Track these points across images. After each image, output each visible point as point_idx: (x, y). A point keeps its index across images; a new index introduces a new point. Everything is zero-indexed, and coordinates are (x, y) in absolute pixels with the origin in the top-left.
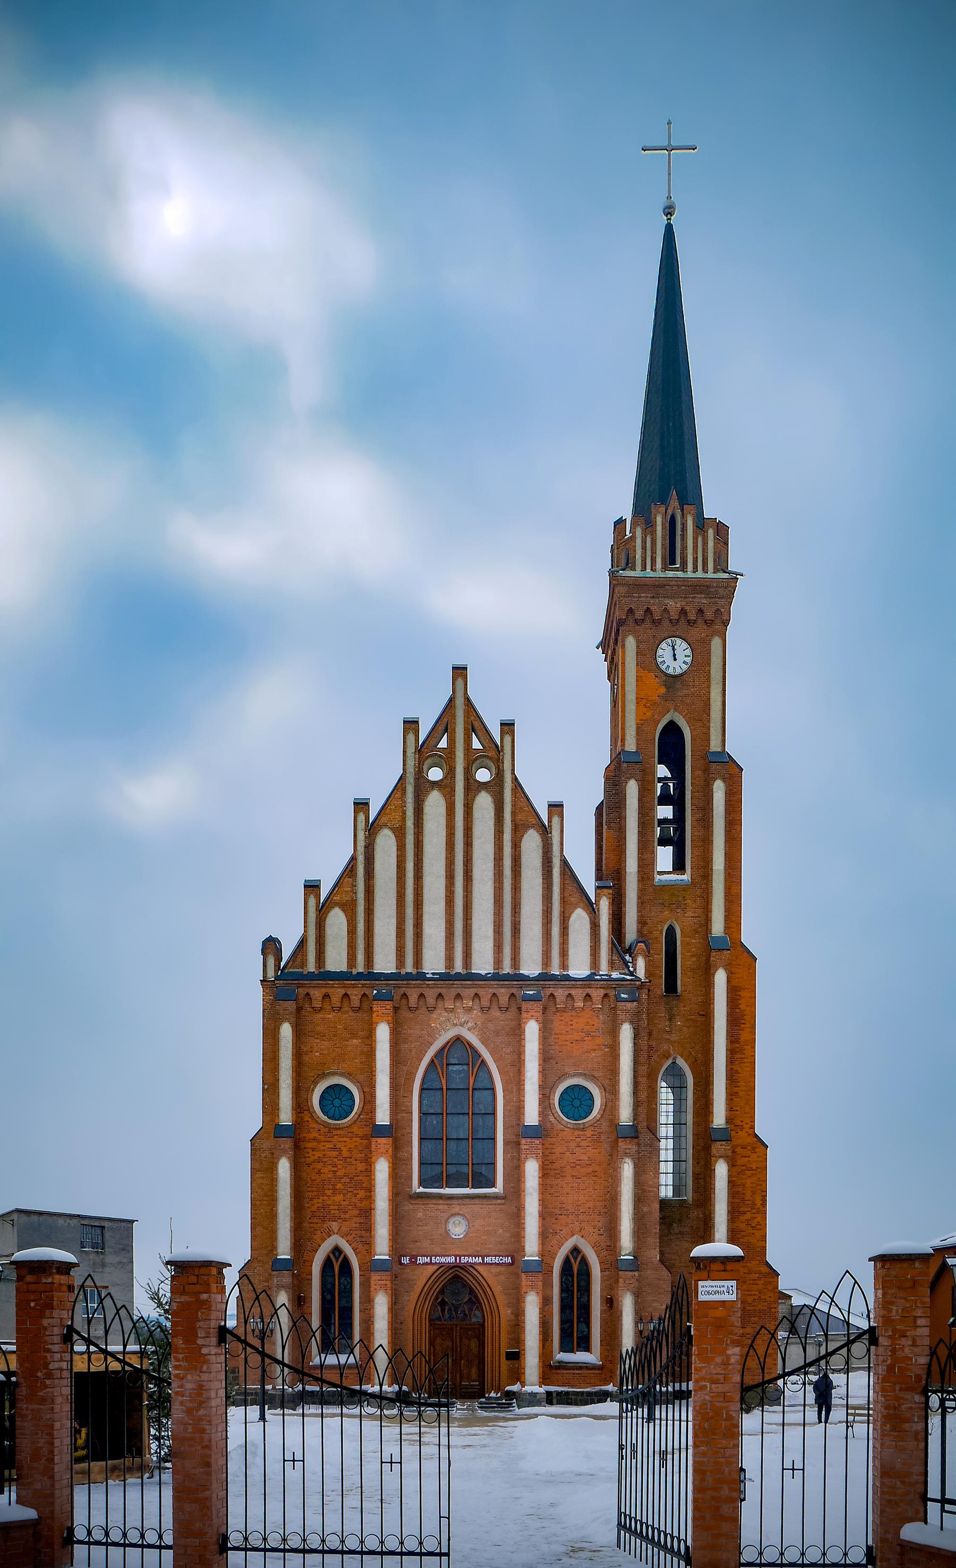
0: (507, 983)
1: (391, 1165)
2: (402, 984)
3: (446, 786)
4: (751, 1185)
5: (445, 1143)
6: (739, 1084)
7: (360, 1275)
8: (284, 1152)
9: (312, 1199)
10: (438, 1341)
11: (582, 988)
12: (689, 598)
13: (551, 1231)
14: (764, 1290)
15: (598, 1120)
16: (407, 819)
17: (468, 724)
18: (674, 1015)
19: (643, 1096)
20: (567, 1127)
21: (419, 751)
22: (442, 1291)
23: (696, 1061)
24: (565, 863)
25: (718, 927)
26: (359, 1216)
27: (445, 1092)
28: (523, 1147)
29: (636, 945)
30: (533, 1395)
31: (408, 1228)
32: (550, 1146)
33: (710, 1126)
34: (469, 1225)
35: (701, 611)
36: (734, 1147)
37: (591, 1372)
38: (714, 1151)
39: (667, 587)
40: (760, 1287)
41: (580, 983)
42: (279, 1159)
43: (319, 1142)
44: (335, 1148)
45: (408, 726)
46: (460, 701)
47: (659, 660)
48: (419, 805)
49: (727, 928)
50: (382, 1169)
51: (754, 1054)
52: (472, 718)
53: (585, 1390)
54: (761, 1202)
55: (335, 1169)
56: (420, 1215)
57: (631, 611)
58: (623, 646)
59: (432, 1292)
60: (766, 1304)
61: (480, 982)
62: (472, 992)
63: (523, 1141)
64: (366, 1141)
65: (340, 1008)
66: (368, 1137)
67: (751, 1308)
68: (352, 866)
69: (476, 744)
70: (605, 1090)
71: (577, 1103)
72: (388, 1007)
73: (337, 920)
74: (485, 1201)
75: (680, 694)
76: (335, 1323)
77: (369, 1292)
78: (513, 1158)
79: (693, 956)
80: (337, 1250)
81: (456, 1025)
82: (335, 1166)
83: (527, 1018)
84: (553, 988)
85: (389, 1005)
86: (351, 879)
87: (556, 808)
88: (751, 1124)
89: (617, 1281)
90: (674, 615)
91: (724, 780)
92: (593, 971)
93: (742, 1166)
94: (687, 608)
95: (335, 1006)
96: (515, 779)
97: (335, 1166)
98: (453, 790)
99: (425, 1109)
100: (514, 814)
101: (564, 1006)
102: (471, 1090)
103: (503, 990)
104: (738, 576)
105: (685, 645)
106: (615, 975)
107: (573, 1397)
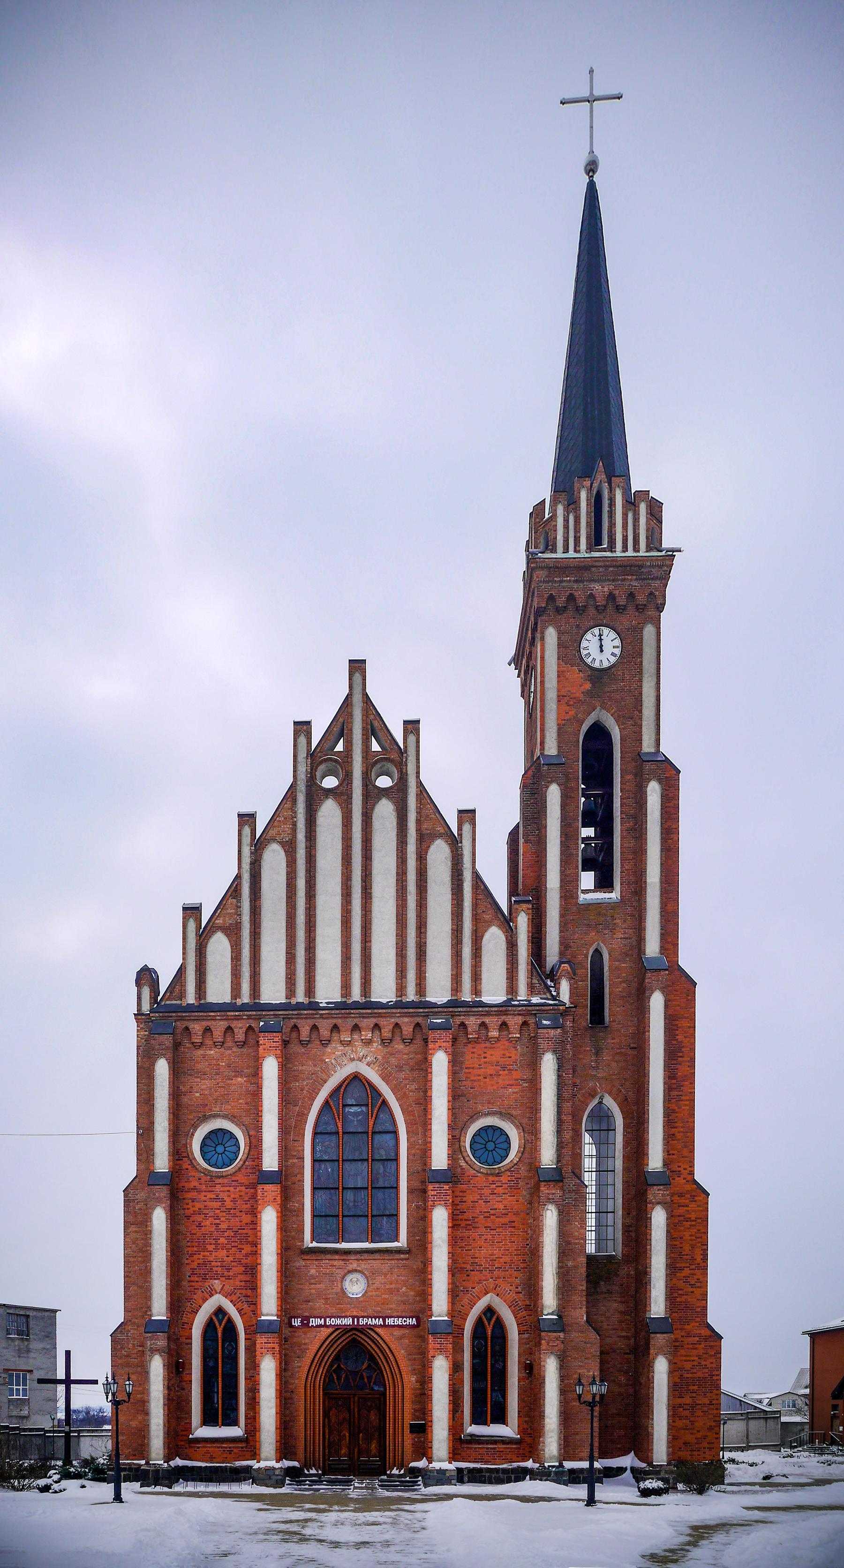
0: (411, 1010)
1: (279, 1214)
2: (293, 1014)
3: (342, 794)
4: (690, 1238)
5: (341, 1193)
6: (677, 1125)
7: (246, 1339)
8: (159, 1201)
9: (192, 1255)
10: (333, 1412)
11: (495, 1015)
12: (618, 580)
13: (462, 1289)
14: (704, 1356)
15: (516, 1164)
16: (298, 830)
17: (367, 724)
18: (602, 1049)
19: (568, 1135)
20: (480, 1173)
21: (312, 755)
22: (337, 1358)
23: (627, 1099)
24: (477, 877)
25: (652, 947)
26: (245, 1273)
27: (341, 1136)
28: (431, 1193)
29: (560, 966)
30: (442, 1472)
31: (300, 1286)
32: (461, 1194)
33: (645, 1170)
34: (368, 1283)
35: (631, 596)
36: (672, 1195)
37: (508, 1446)
38: (650, 1197)
39: (593, 569)
40: (701, 1352)
41: (496, 1009)
42: (153, 1209)
43: (199, 1191)
44: (217, 1199)
45: (299, 727)
46: (357, 699)
47: (584, 652)
48: (311, 816)
49: (663, 949)
50: (269, 1219)
51: (693, 1090)
52: (372, 717)
53: (501, 1467)
55: (217, 1221)
56: (313, 1272)
57: (551, 598)
58: (543, 639)
59: (326, 1358)
60: (706, 1370)
61: (380, 1011)
62: (372, 1021)
63: (430, 1187)
65: (223, 1043)
66: (253, 1186)
67: (690, 1375)
68: (237, 885)
69: (375, 747)
70: (523, 1130)
71: (491, 1146)
72: (276, 1039)
73: (219, 946)
74: (387, 1256)
75: (607, 689)
77: (255, 1356)
78: (418, 1207)
79: (623, 982)
80: (220, 1311)
81: (352, 1060)
82: (218, 1218)
83: (434, 1049)
84: (464, 1015)
85: (277, 1037)
86: (235, 900)
87: (467, 816)
88: (690, 1169)
89: (538, 1344)
90: (600, 601)
91: (660, 781)
92: (510, 997)
93: (679, 1216)
94: (617, 592)
95: (217, 1040)
96: (420, 784)
97: (218, 1218)
98: (350, 798)
99: (318, 1156)
100: (418, 822)
101: (477, 1036)
102: (370, 1134)
103: (406, 1020)
104: (674, 554)
105: (613, 635)
106: (535, 1000)
107: (487, 1475)
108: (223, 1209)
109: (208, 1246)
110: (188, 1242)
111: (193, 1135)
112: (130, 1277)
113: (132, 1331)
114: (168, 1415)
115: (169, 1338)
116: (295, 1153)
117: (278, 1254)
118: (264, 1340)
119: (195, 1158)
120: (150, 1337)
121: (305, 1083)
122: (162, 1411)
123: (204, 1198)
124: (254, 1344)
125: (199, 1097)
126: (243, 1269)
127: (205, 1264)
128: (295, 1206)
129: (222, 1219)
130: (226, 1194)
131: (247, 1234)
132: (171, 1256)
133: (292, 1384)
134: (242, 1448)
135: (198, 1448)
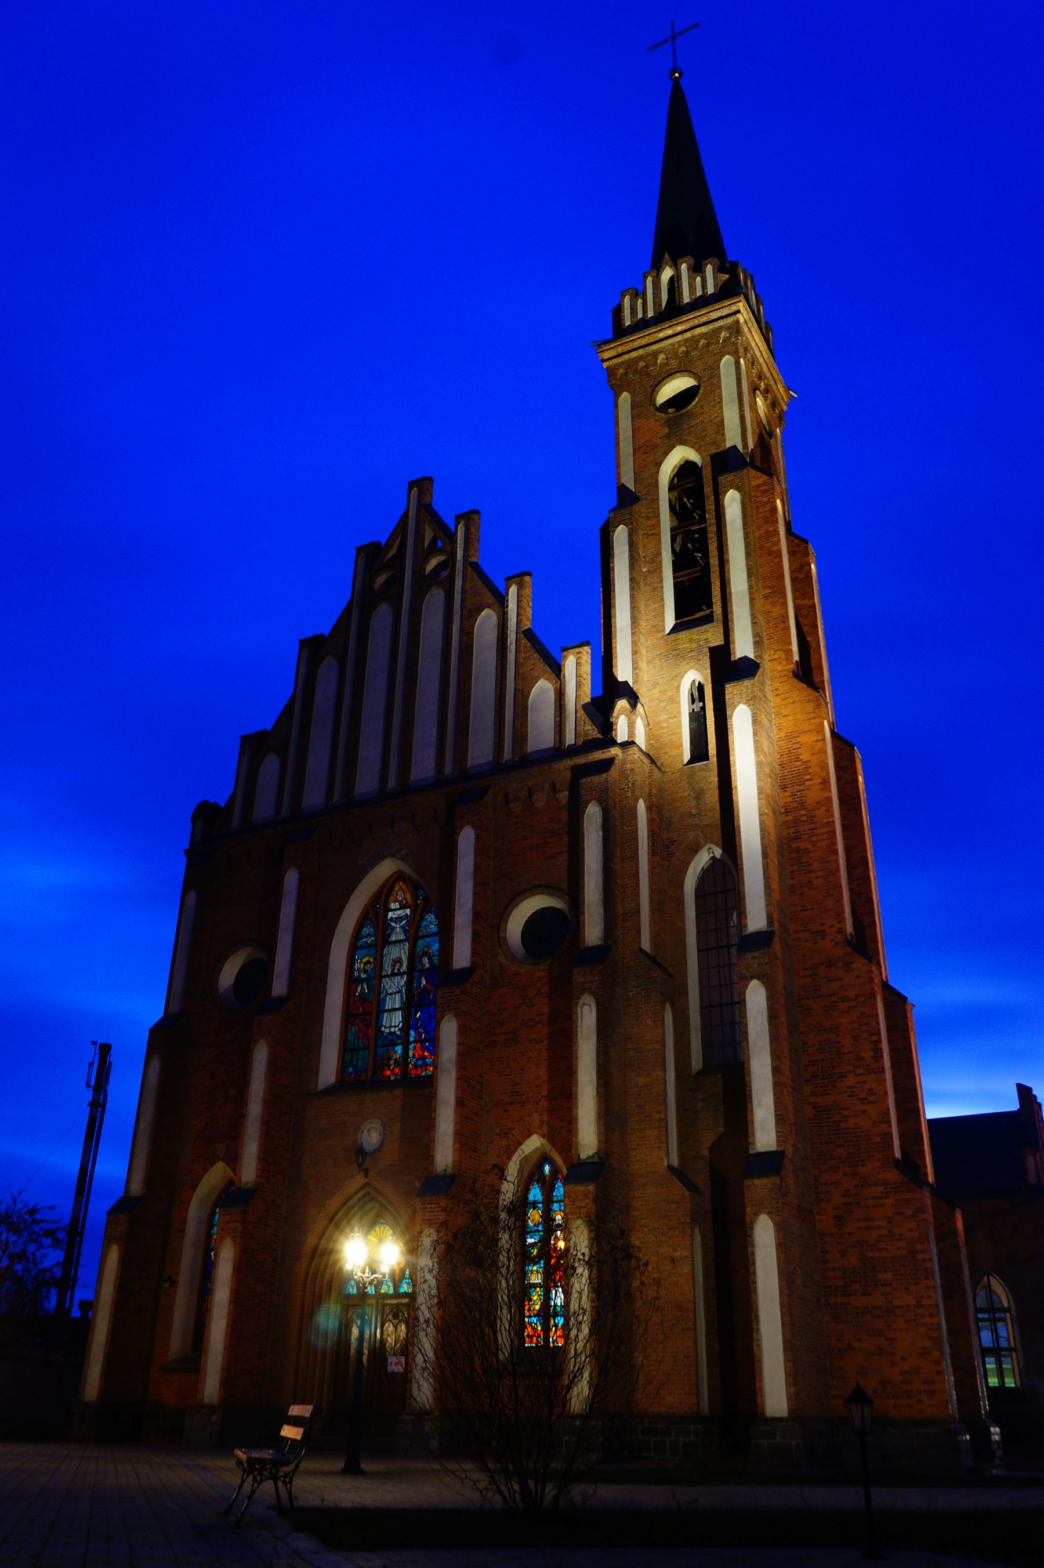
54: (872, 1054)
60: (904, 1244)
88: (840, 925)
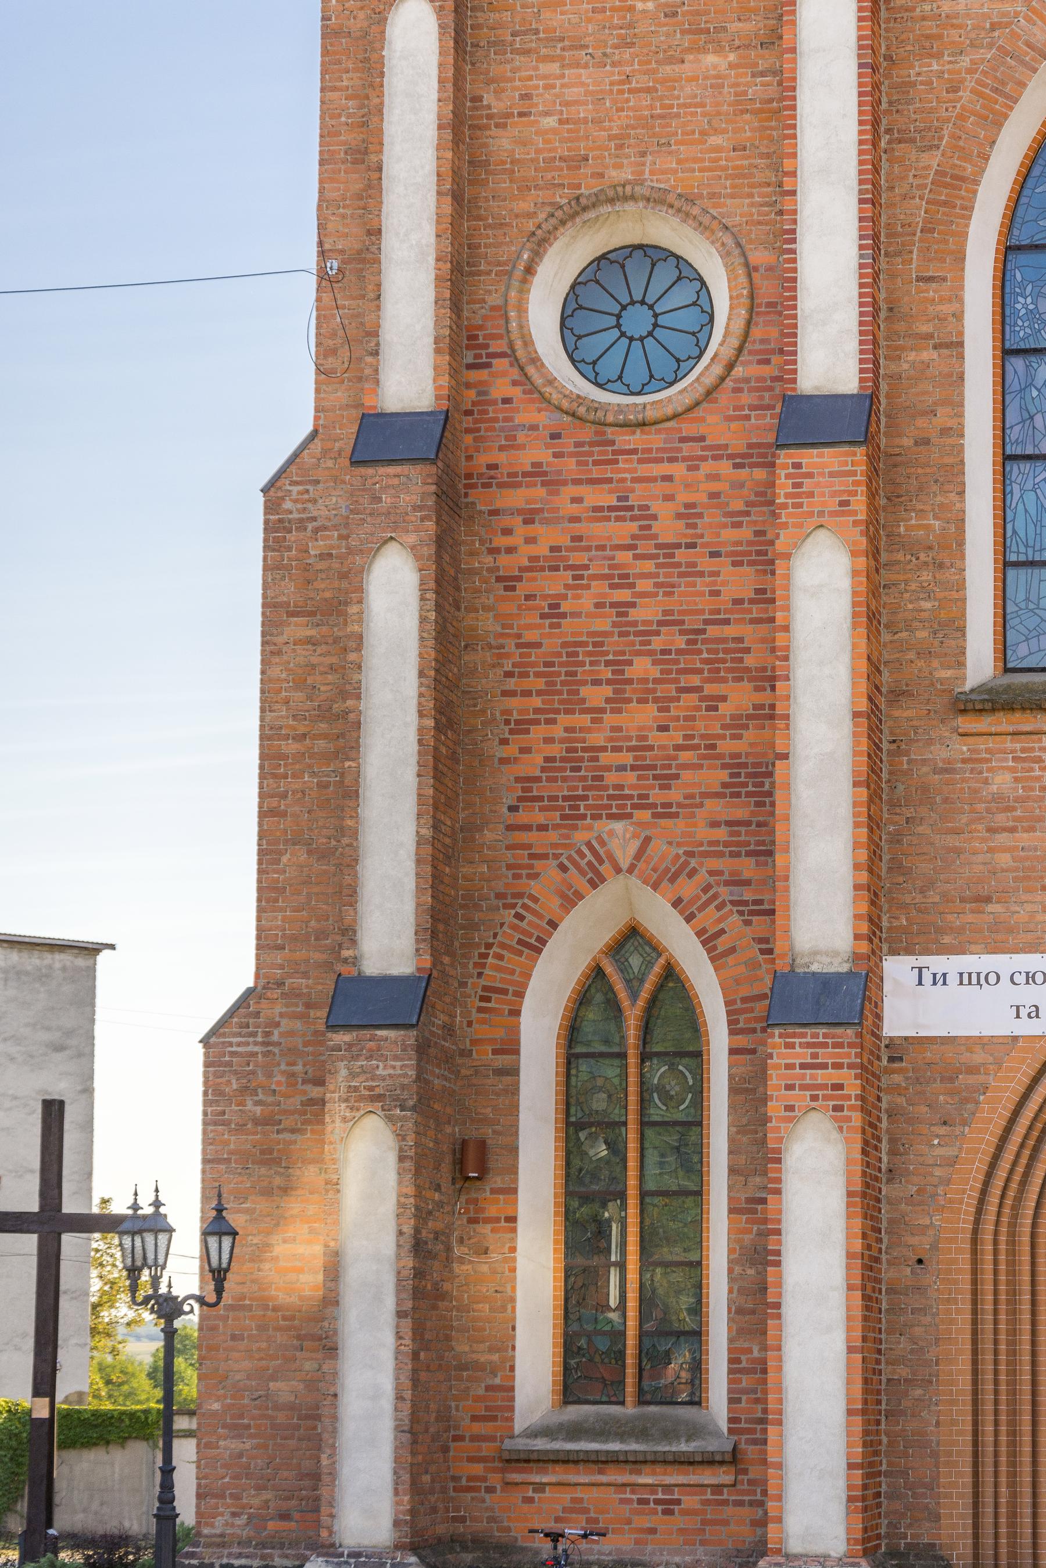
7: (732, 1051)
9: (522, 727)
26: (730, 791)
31: (952, 841)
44: (622, 509)
55: (623, 595)
56: (1001, 782)
64: (760, 474)
76: (622, 1266)
77: (765, 1120)
82: (625, 581)
97: (625, 581)
99: (1021, 335)
108: (646, 547)
109: (585, 691)
110: (509, 674)
111: (530, 270)
112: (284, 814)
113: (285, 1024)
114: (415, 1356)
115: (422, 1049)
116: (925, 328)
117: (856, 715)
118: (802, 1054)
119: (536, 360)
120: (350, 1046)
121: (965, 62)
122: (388, 1338)
123: (574, 509)
124: (761, 1074)
125: (554, 131)
126: (724, 775)
127: (572, 759)
128: (928, 527)
129: (644, 585)
130: (659, 488)
131: (740, 640)
132: (438, 728)
133: (923, 1229)
134: (717, 1488)
135: (540, 1487)
